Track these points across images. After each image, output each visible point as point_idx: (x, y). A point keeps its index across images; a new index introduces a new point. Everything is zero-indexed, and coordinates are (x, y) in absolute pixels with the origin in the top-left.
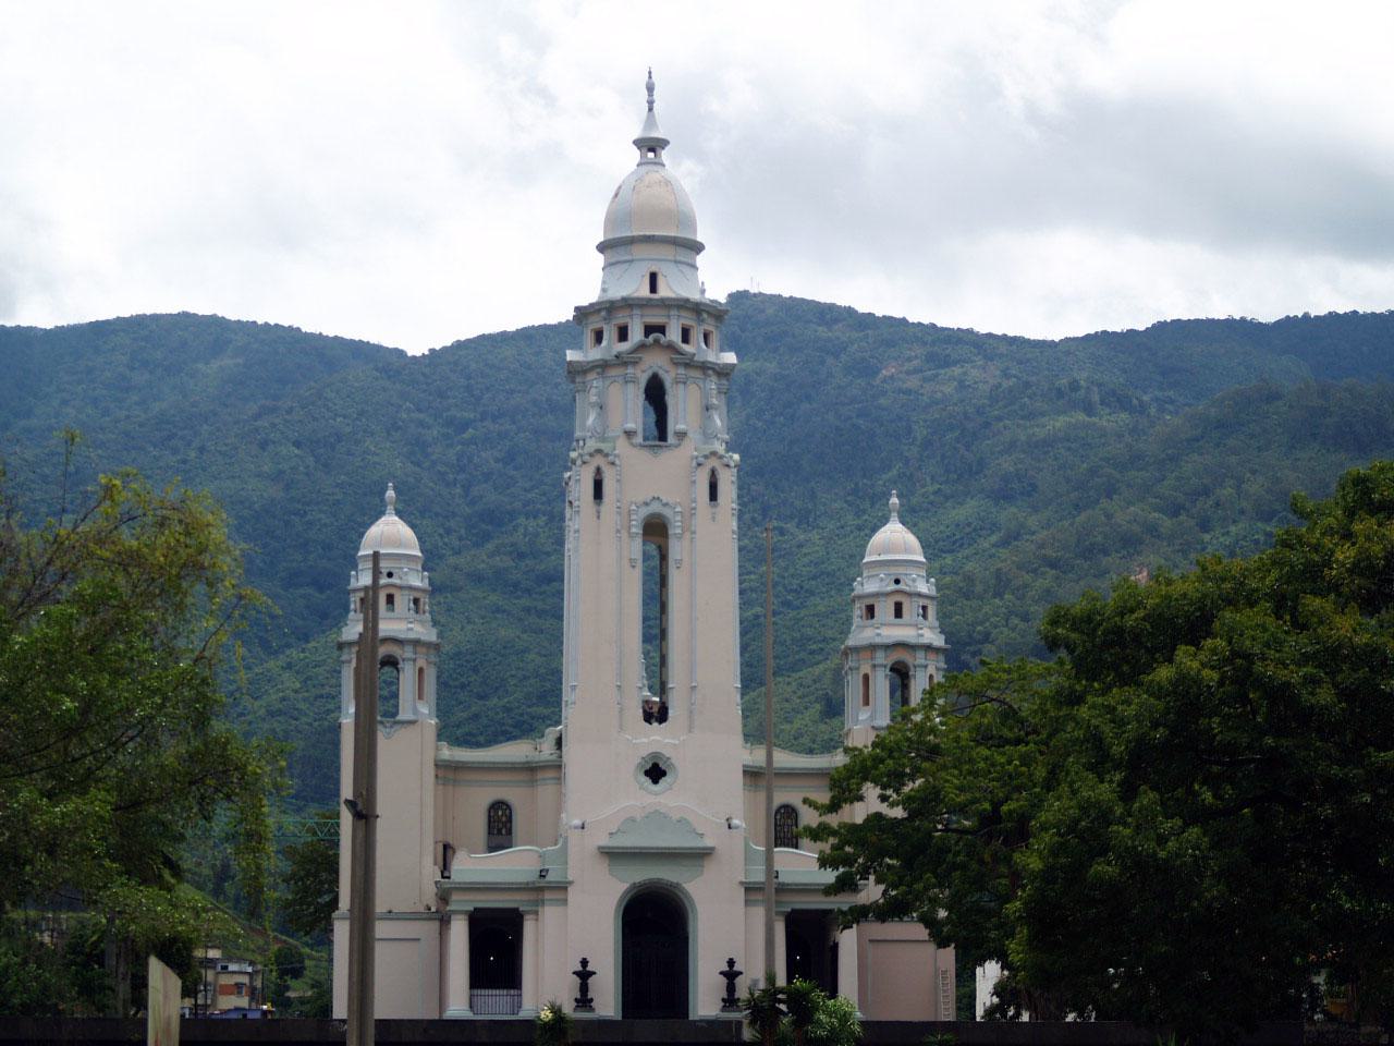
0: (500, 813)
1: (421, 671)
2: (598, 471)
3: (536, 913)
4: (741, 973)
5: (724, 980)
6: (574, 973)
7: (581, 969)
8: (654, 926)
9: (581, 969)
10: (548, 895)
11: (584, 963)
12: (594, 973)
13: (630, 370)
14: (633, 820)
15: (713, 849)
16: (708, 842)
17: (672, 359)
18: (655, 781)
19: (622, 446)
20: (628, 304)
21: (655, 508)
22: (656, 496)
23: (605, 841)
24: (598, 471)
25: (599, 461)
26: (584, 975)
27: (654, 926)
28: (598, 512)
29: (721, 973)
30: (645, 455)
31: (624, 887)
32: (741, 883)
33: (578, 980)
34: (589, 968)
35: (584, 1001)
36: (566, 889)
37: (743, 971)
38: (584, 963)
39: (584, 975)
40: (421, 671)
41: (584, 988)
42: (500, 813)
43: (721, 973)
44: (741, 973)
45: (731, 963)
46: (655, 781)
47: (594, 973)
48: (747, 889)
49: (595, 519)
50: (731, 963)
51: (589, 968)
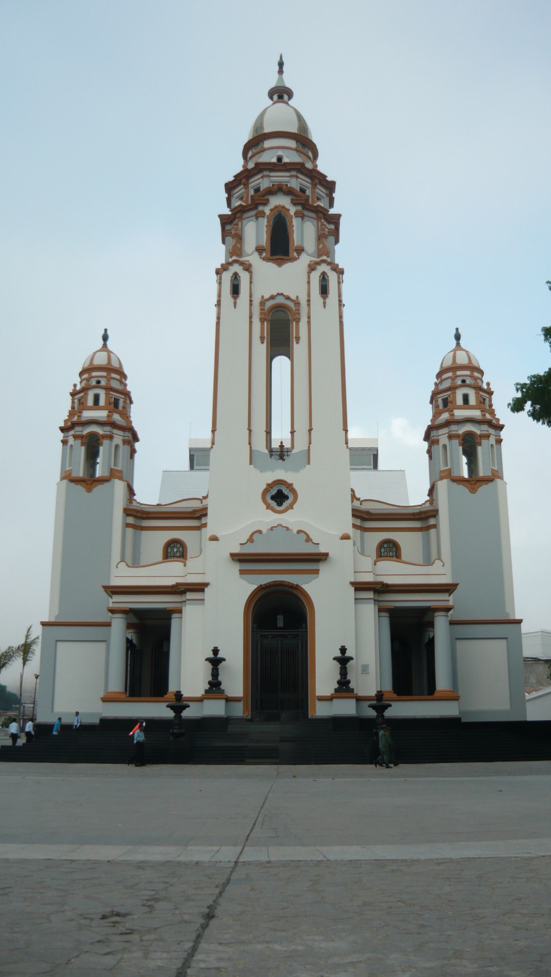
0: (175, 550)
1: (117, 447)
2: (236, 276)
3: (180, 611)
4: (352, 659)
5: (337, 665)
6: (207, 660)
7: (212, 656)
8: (279, 619)
9: (211, 655)
10: (189, 596)
11: (216, 651)
12: (224, 660)
13: (261, 208)
14: (260, 532)
15: (326, 555)
16: (322, 549)
17: (292, 201)
18: (280, 504)
19: (255, 260)
20: (260, 168)
21: (280, 300)
22: (280, 293)
23: (237, 550)
24: (236, 276)
25: (236, 268)
26: (215, 661)
27: (279, 619)
28: (235, 304)
29: (335, 659)
30: (271, 266)
31: (253, 587)
32: (352, 584)
33: (209, 666)
34: (220, 655)
35: (215, 687)
36: (203, 590)
37: (354, 656)
38: (216, 651)
39: (215, 661)
40: (117, 447)
41: (215, 673)
42: (175, 550)
43: (335, 659)
44: (352, 659)
45: (343, 650)
46: (280, 504)
47: (224, 660)
48: (356, 589)
49: (233, 307)
50: (343, 650)
51: (220, 655)
